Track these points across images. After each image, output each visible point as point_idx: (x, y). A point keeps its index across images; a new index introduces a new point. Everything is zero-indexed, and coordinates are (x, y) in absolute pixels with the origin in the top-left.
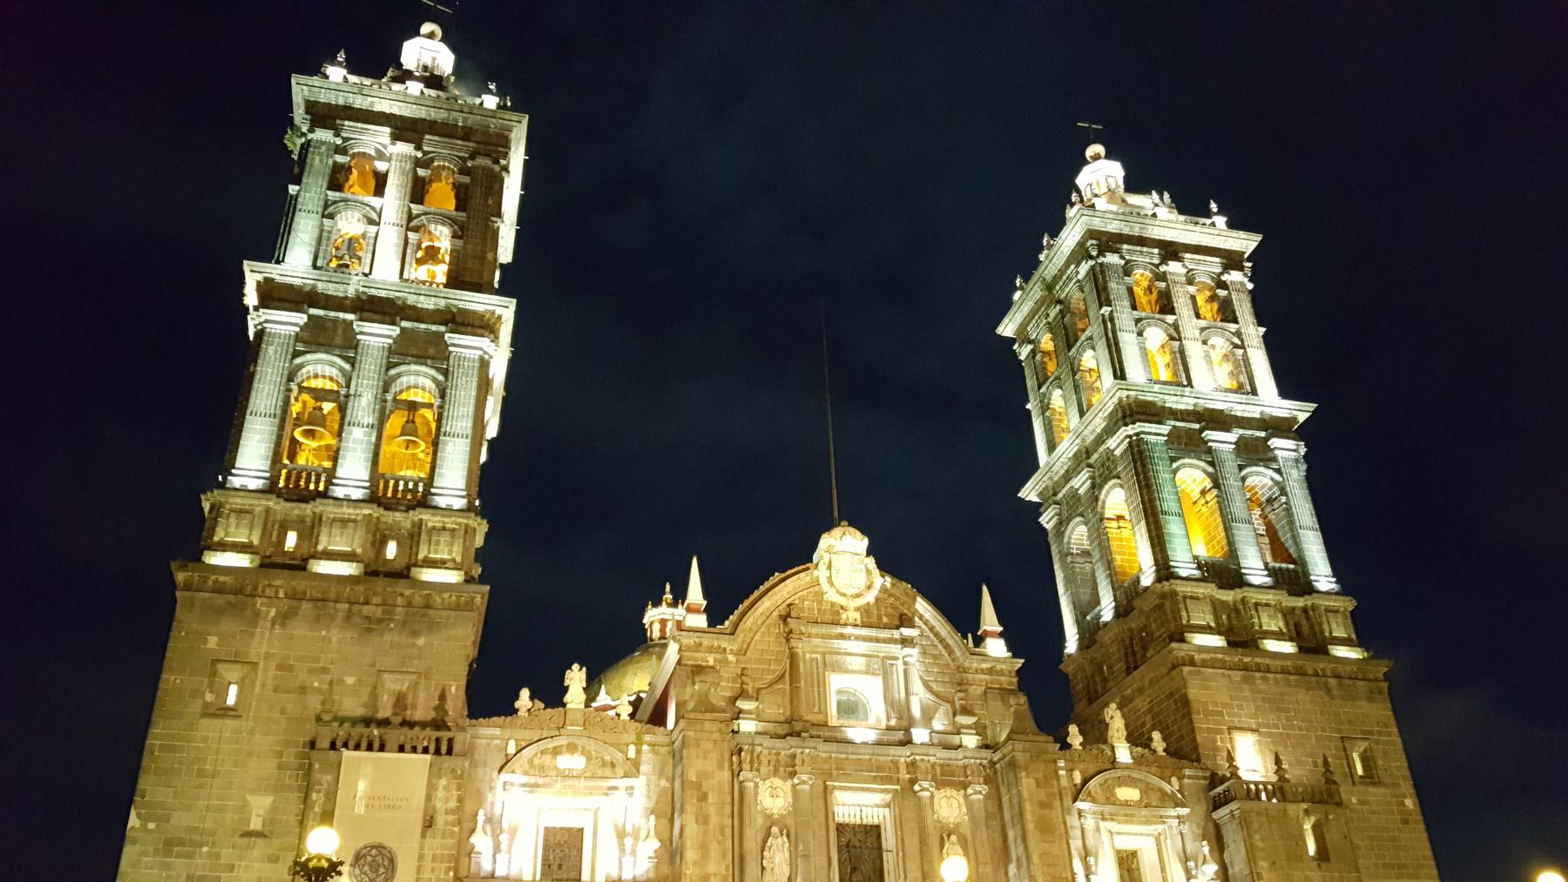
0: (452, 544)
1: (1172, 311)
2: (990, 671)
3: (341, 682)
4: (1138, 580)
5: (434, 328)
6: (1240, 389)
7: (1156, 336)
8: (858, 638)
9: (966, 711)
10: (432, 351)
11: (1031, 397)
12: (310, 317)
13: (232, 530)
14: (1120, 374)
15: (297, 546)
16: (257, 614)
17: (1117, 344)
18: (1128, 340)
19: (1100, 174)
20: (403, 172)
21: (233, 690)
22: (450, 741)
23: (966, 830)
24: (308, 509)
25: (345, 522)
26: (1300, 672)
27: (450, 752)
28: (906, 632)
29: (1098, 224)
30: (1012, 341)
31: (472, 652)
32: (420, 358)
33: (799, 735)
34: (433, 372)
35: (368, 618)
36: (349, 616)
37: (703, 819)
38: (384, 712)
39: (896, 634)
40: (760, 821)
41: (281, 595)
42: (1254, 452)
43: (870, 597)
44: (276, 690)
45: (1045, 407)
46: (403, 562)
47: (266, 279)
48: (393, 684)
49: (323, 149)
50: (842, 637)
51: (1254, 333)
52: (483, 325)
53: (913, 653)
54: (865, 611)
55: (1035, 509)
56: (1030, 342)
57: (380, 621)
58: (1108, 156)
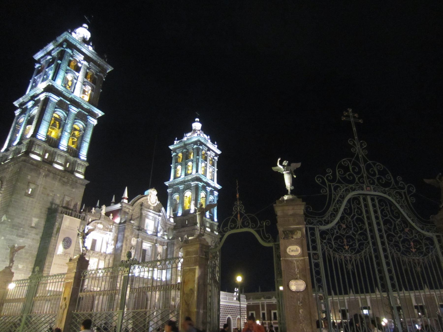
0: (82, 168)
1: (206, 161)
2: (170, 224)
3: (56, 195)
4: (189, 210)
5: (85, 113)
6: (211, 179)
7: (203, 165)
8: (153, 213)
9: (165, 231)
10: (84, 119)
11: (173, 164)
12: (61, 100)
13: (36, 149)
14: (197, 171)
15: (48, 157)
16: (40, 173)
17: (198, 164)
18: (200, 164)
19: (197, 125)
20: (84, 69)
21: (31, 190)
22: (84, 217)
23: (161, 254)
24: (53, 149)
25: (61, 156)
26: (210, 235)
27: (84, 220)
28: (161, 214)
29: (201, 139)
30: (171, 150)
31: (82, 195)
32: (82, 120)
33: (141, 230)
34: (83, 124)
35: (63, 181)
36: (60, 180)
37: (126, 245)
38: (64, 205)
39: (158, 213)
40: (130, 246)
41: (46, 170)
42: (212, 193)
43: (155, 205)
44: (42, 193)
45: (175, 168)
46: (70, 169)
47: (52, 85)
48: (67, 199)
49: (68, 54)
50: (149, 212)
51: (216, 170)
52: (93, 115)
53: (160, 218)
54: (154, 207)
55: (167, 187)
56: (176, 153)
57: (66, 183)
58: (200, 122)
